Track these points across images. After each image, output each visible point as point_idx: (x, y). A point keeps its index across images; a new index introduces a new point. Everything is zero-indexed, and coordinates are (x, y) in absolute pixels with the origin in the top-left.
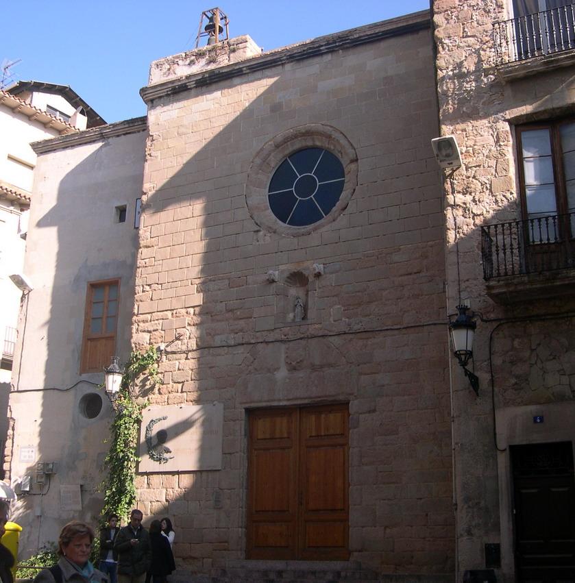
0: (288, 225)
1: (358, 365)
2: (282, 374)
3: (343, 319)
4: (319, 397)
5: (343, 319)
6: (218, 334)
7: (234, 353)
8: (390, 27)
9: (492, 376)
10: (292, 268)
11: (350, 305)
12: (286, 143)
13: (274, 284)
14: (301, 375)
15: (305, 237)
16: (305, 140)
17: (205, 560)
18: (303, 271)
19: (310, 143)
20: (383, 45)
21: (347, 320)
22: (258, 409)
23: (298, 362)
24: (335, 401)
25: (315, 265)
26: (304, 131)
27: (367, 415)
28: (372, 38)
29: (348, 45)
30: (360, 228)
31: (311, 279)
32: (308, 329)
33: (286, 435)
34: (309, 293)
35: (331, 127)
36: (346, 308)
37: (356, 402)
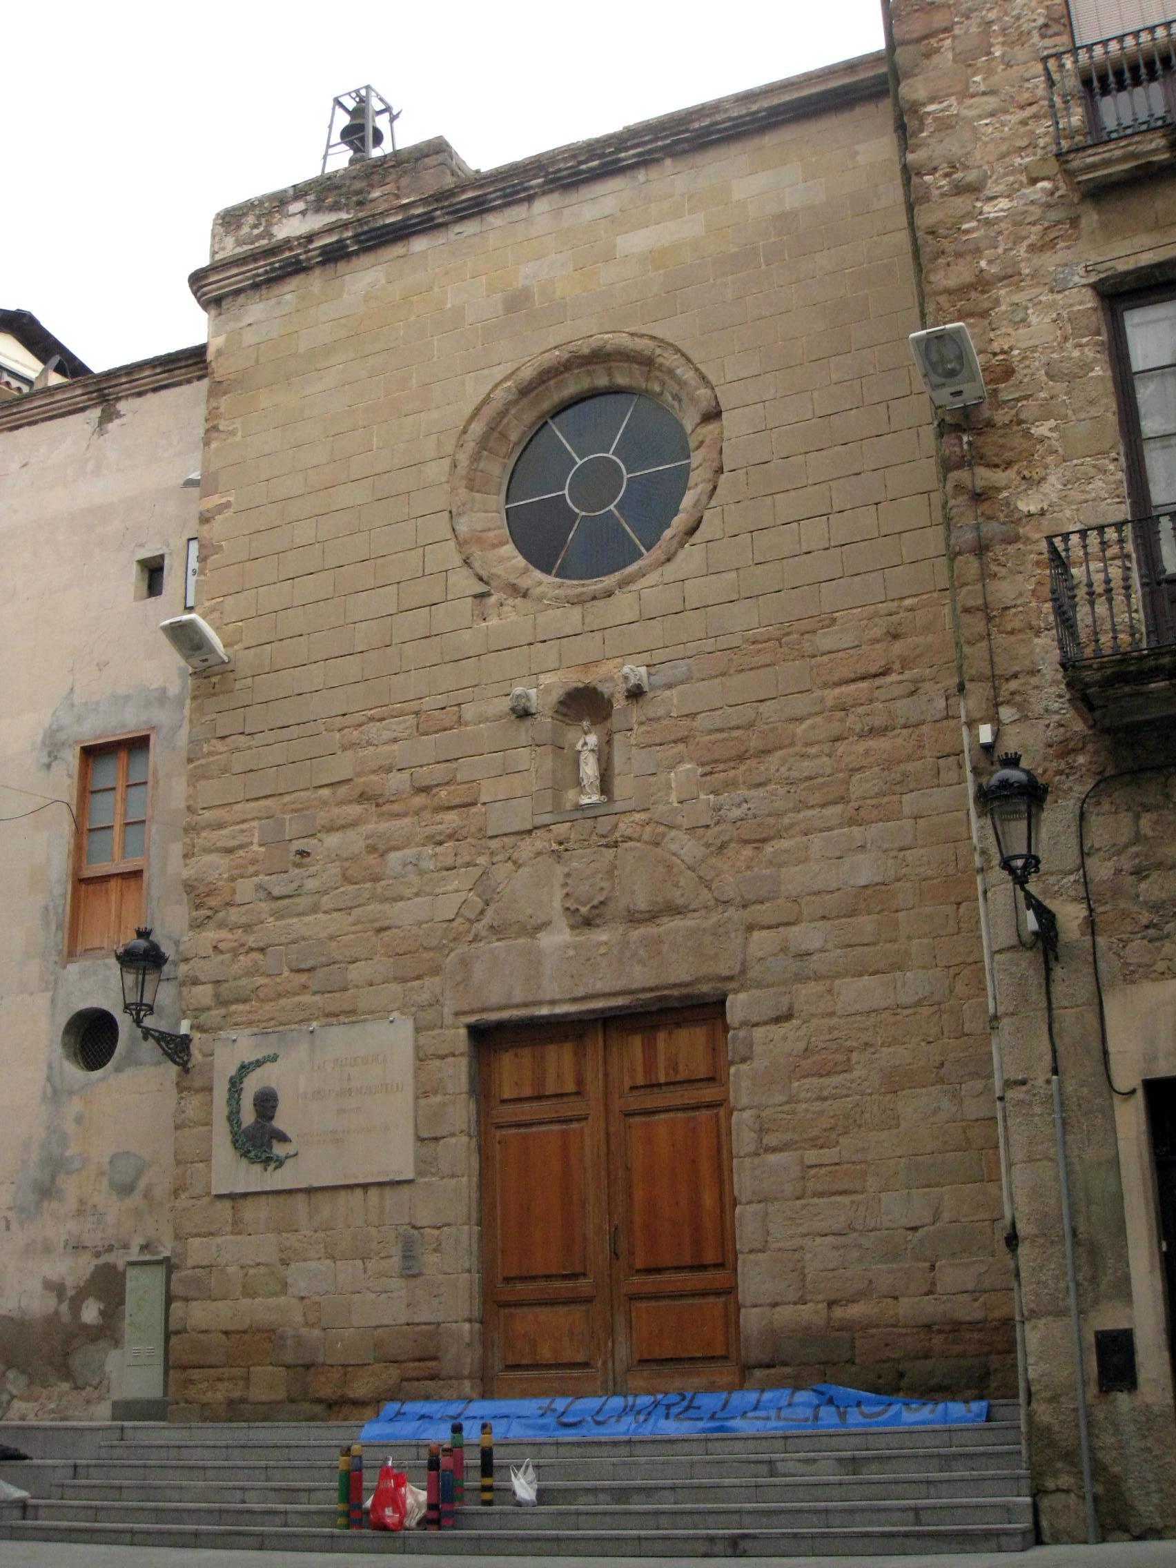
0: (558, 580)
1: (744, 907)
2: (558, 937)
3: (703, 797)
4: (651, 990)
5: (703, 797)
7: (438, 891)
8: (786, 98)
9: (1091, 910)
10: (576, 679)
11: (715, 761)
12: (544, 382)
13: (529, 721)
14: (604, 937)
15: (599, 604)
16: (590, 373)
18: (600, 688)
19: (602, 381)
20: (769, 140)
21: (712, 797)
22: (500, 1026)
23: (594, 907)
24: (687, 996)
25: (626, 669)
26: (586, 351)
27: (773, 1028)
28: (743, 124)
29: (685, 146)
30: (733, 574)
31: (619, 703)
32: (616, 826)
33: (570, 1087)
34: (616, 737)
35: (653, 338)
36: (708, 769)
37: (742, 996)
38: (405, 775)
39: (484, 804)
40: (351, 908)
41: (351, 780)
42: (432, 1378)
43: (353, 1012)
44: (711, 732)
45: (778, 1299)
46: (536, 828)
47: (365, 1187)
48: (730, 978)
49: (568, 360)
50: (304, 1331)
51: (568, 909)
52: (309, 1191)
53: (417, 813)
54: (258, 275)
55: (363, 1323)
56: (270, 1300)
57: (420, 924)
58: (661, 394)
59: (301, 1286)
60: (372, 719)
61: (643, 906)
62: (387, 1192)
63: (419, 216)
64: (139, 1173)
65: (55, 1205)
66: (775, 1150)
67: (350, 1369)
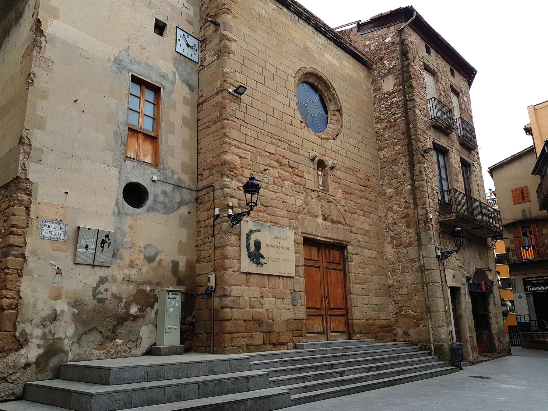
2: (320, 220)
4: (337, 240)
6: (286, 180)
7: (296, 197)
16: (316, 80)
18: (325, 162)
26: (319, 75)
29: (337, 42)
31: (327, 168)
35: (331, 83)
36: (343, 193)
37: (351, 247)
38: (287, 160)
39: (305, 178)
40: (276, 192)
41: (274, 154)
42: (300, 336)
45: (360, 318)
46: (315, 190)
47: (283, 277)
48: (349, 242)
49: (316, 74)
50: (268, 320)
51: (323, 214)
52: (269, 276)
53: (290, 173)
55: (284, 319)
56: (259, 310)
59: (267, 306)
60: (279, 139)
61: (335, 220)
62: (288, 279)
63: (289, 3)
64: (156, 255)
65: (118, 261)
66: (357, 284)
67: (280, 333)
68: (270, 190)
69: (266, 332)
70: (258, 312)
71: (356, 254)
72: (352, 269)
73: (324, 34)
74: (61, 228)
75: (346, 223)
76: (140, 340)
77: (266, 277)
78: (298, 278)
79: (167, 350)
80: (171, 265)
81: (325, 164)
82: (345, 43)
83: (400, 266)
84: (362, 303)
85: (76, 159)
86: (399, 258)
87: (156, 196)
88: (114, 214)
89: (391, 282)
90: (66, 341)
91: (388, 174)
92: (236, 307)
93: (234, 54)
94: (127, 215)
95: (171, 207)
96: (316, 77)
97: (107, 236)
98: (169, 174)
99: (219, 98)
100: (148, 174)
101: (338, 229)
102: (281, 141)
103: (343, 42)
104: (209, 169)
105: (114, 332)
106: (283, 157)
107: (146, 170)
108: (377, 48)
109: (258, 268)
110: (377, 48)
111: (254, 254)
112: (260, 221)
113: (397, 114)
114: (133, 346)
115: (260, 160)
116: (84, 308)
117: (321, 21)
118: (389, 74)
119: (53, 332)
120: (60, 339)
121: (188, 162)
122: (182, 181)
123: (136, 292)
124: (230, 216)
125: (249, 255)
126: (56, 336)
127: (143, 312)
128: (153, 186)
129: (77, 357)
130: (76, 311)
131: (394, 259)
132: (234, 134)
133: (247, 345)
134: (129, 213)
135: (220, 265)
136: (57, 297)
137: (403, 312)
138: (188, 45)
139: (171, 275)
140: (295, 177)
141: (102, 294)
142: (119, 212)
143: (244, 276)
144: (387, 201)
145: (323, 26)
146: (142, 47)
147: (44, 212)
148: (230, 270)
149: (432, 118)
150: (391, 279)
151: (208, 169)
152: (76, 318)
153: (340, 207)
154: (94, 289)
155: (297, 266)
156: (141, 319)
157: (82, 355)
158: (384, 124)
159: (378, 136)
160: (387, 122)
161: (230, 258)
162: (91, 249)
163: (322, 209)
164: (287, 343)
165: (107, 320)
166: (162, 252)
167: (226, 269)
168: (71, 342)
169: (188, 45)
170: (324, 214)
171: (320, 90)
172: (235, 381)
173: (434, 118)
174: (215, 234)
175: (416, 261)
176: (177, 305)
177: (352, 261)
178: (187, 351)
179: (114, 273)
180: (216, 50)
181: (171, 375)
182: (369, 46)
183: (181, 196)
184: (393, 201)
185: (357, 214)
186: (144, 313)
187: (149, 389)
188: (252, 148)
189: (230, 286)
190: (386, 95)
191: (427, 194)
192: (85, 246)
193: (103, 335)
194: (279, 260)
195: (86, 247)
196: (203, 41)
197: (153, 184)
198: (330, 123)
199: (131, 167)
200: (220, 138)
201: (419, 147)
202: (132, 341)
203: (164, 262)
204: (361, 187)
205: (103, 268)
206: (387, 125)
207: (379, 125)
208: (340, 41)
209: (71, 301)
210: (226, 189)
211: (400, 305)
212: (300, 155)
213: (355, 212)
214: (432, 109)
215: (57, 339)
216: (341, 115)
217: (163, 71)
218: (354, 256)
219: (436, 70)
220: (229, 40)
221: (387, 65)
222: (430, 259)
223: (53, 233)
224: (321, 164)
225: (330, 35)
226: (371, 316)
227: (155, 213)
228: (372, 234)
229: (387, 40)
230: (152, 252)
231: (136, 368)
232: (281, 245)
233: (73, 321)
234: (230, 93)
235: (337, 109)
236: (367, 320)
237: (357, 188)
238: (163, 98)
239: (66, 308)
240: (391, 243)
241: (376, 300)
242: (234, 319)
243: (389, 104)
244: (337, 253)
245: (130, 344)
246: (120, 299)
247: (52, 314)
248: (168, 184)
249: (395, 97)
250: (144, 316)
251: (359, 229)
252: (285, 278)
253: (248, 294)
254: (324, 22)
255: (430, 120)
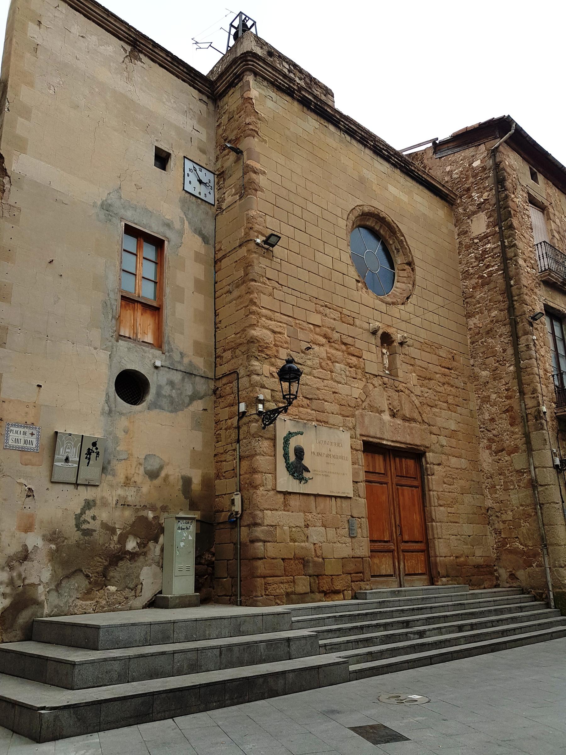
2: (386, 417)
6: (337, 362)
16: (376, 223)
17: (345, 592)
18: (391, 335)
29: (405, 170)
31: (395, 344)
35: (398, 227)
37: (431, 454)
38: (338, 335)
39: (364, 359)
40: (324, 379)
42: (362, 580)
43: (327, 422)
44: (419, 366)
45: (446, 555)
47: (336, 497)
48: (428, 447)
49: (376, 214)
50: (316, 559)
51: (390, 409)
52: (316, 496)
53: (343, 352)
54: (277, 81)
55: (339, 556)
56: (303, 544)
57: (347, 396)
58: (392, 244)
59: (314, 538)
60: (326, 306)
61: (408, 416)
62: (343, 500)
63: (337, 118)
64: (161, 468)
65: (110, 477)
66: (441, 506)
67: (333, 577)
68: (315, 377)
69: (314, 575)
70: (302, 548)
71: (439, 464)
72: (434, 486)
73: (387, 159)
74: (32, 434)
75: (423, 421)
76: (140, 586)
77: (312, 498)
78: (358, 498)
79: (177, 601)
80: (181, 483)
81: (392, 338)
82: (416, 170)
83: (502, 481)
84: (449, 533)
85: (52, 341)
86: (500, 468)
87: (159, 387)
88: (103, 413)
89: (489, 503)
90: (41, 589)
91: (482, 350)
92: (270, 539)
93: (262, 191)
94: (121, 414)
95: (181, 402)
96: (378, 219)
97: (94, 444)
98: (177, 357)
99: (243, 251)
100: (149, 358)
101: (412, 429)
102: (330, 308)
103: (413, 168)
104: (231, 349)
105: (105, 576)
106: (333, 329)
107: (145, 353)
108: (462, 176)
109: (301, 485)
110: (462, 176)
111: (294, 466)
112: (302, 419)
113: (493, 266)
114: (131, 595)
115: (301, 336)
116: (65, 543)
117: (382, 141)
118: (479, 211)
119: (23, 576)
120: (33, 585)
121: (202, 340)
122: (195, 366)
123: (134, 520)
124: (260, 413)
125: (288, 468)
126: (27, 582)
127: (144, 547)
128: (155, 374)
129: (56, 610)
130: (53, 547)
131: (494, 470)
132: (265, 300)
133: (288, 594)
134: (124, 412)
135: (248, 482)
136: (28, 528)
137: (508, 546)
138: (200, 182)
139: (182, 497)
140: (351, 357)
141: (89, 523)
142: (110, 411)
143: (281, 497)
144: (480, 389)
145: (385, 149)
146: (138, 186)
147: (10, 413)
148: (261, 488)
149: (542, 271)
150: (489, 499)
151: (229, 350)
152: (53, 556)
153: (414, 398)
154: (78, 517)
155: (355, 482)
156: (142, 557)
157: (61, 607)
158: (474, 281)
159: (466, 297)
160: (478, 278)
161: (262, 472)
162: (74, 462)
163: (389, 402)
164: (343, 591)
165: (95, 559)
166: (168, 464)
167: (256, 487)
168: (47, 590)
169: (200, 182)
170: (392, 409)
171: (382, 236)
172: (271, 645)
173: (545, 270)
174: (240, 438)
175: (525, 472)
176: (190, 538)
177: (433, 474)
178: (204, 601)
179: (105, 494)
180: (238, 186)
181: (182, 636)
182: (450, 173)
183: (194, 388)
184: (489, 388)
185: (438, 407)
186: (145, 550)
187: (152, 655)
188: (290, 319)
189: (262, 511)
190: (476, 241)
191: (537, 377)
192: (64, 458)
193: (90, 580)
194: (329, 474)
195: (67, 460)
196: (221, 175)
197: (156, 371)
198: (398, 282)
199: (126, 349)
200: (246, 307)
201: (524, 311)
202: (129, 588)
203: (171, 478)
204: (443, 369)
205: (89, 488)
206: (478, 281)
207: (467, 283)
208: (410, 168)
209: (47, 533)
210: (255, 377)
211: (503, 536)
212: (356, 326)
213: (436, 405)
214: (541, 258)
215: (28, 585)
216: (413, 270)
217: (167, 217)
218: (436, 467)
219: (546, 203)
220: (255, 173)
221: (476, 198)
222: (545, 470)
223: (22, 442)
224: (386, 339)
225: (395, 159)
226: (462, 552)
227: (158, 410)
228: (460, 436)
229: (475, 164)
230: (154, 465)
231: (134, 627)
232: (332, 453)
233: (50, 561)
234: (258, 244)
235: (406, 261)
236: (457, 557)
237: (437, 371)
238: (167, 255)
239: (40, 543)
240: (489, 448)
241: (468, 529)
242: (268, 557)
243: (481, 252)
244: (411, 463)
245: (127, 592)
246: (113, 530)
247: (22, 551)
248: (175, 371)
249: (489, 242)
250: (145, 554)
251: (442, 429)
252: (338, 500)
253: (288, 522)
254: (387, 143)
255: (539, 274)
